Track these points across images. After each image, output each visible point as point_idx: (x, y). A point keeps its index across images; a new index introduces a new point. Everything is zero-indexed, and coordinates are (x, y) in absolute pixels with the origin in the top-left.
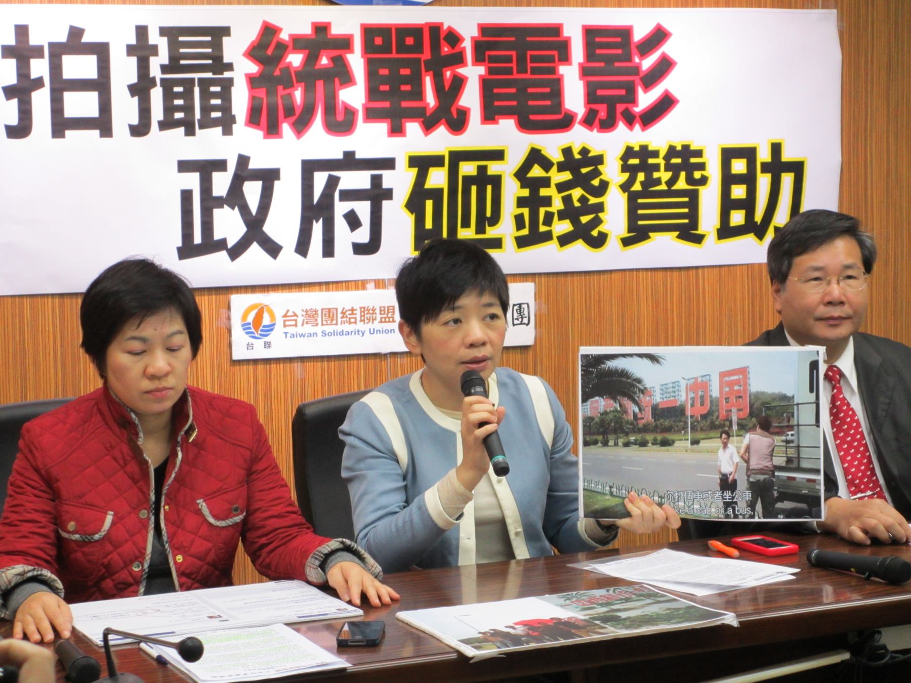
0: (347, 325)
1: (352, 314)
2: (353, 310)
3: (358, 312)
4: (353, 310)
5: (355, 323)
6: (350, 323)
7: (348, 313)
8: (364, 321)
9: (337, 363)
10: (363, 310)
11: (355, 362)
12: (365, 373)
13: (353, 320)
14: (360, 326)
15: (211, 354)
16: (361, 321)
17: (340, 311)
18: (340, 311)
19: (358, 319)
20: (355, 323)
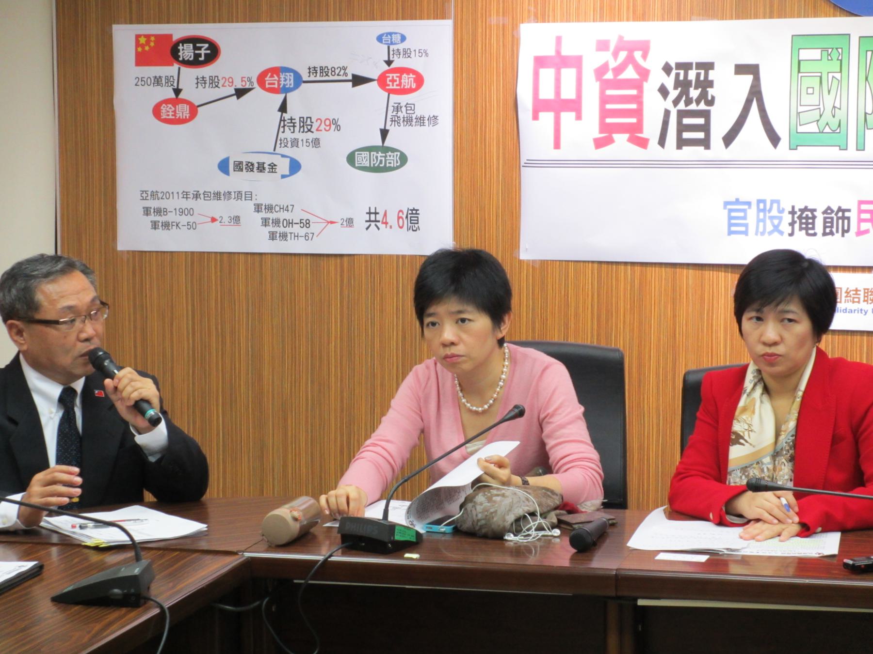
0: (851, 304)
1: (856, 294)
2: (857, 290)
3: (862, 293)
4: (857, 290)
5: (859, 302)
6: (854, 302)
7: (852, 293)
8: (867, 301)
9: (841, 337)
10: (866, 290)
11: (859, 337)
12: (868, 349)
13: (856, 300)
14: (863, 305)
15: (725, 319)
16: (864, 301)
17: (844, 290)
18: (844, 290)
19: (862, 299)
20: (859, 302)
